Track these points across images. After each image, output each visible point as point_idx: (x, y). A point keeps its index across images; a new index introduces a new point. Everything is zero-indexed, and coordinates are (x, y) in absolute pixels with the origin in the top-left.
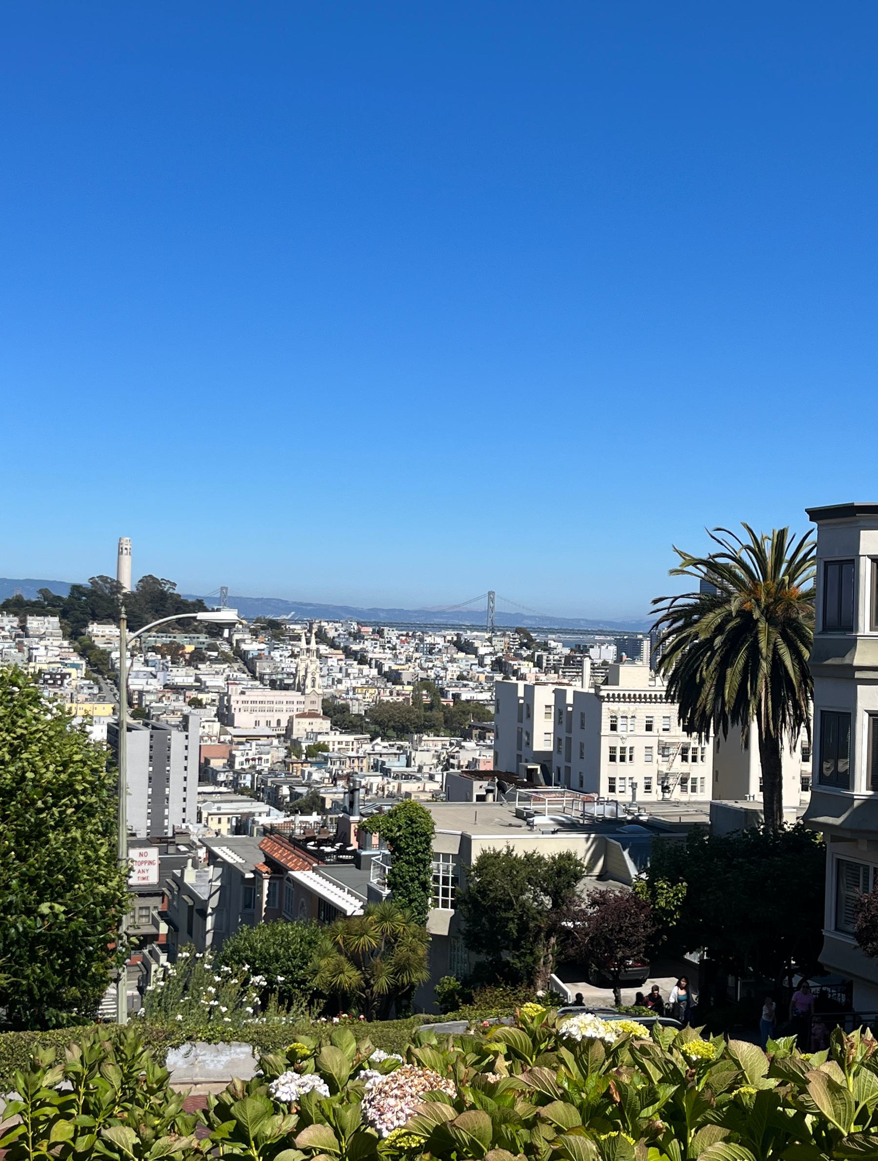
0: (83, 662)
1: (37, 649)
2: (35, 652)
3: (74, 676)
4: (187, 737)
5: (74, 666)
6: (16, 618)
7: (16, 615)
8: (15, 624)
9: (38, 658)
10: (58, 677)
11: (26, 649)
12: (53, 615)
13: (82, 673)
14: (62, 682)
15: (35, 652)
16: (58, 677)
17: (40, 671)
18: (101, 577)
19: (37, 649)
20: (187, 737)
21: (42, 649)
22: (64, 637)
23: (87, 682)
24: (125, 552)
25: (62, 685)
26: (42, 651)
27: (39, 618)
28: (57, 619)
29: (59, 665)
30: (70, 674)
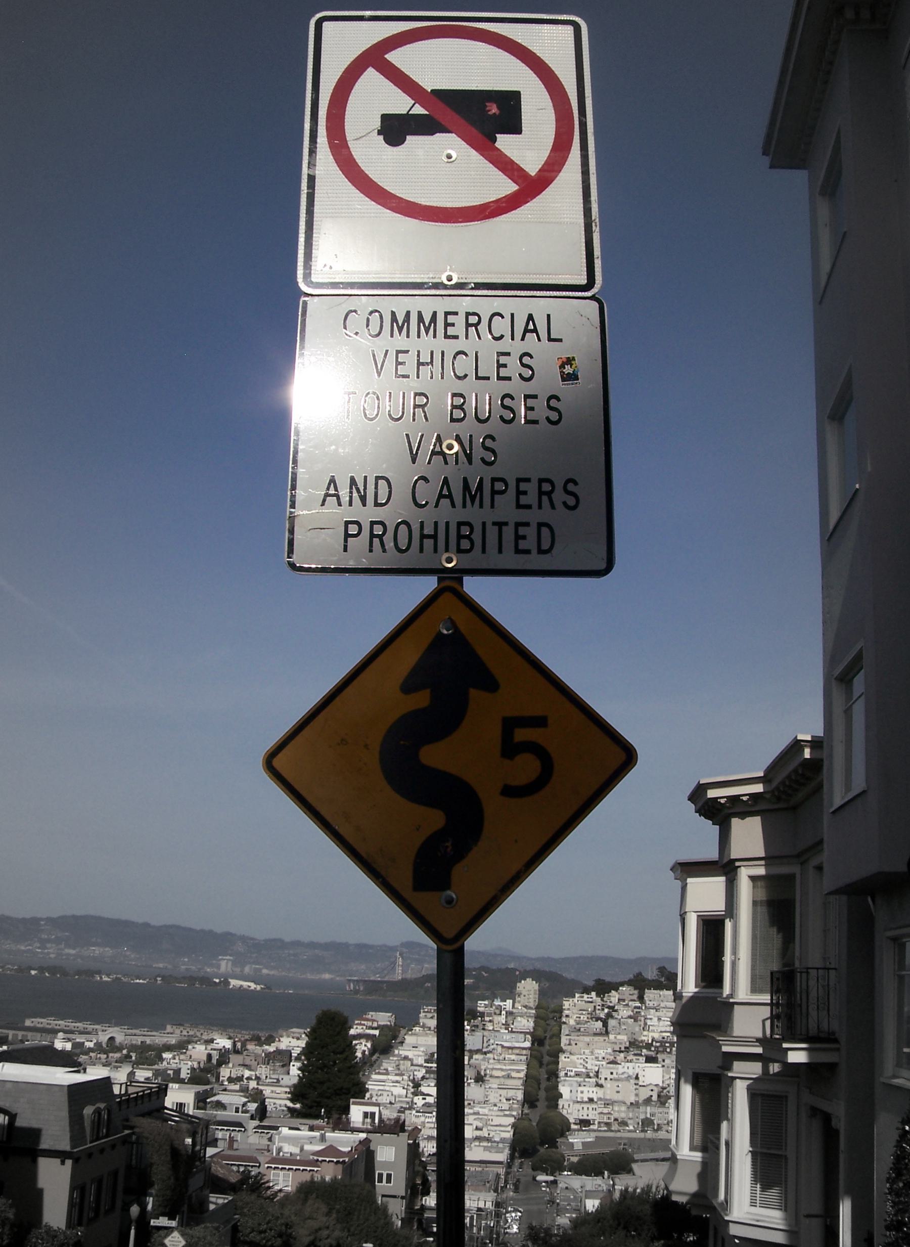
2: (649, 1022)
6: (636, 992)
7: (635, 989)
8: (635, 997)
10: (667, 1045)
11: (643, 1019)
14: (671, 1050)
16: (667, 1045)
17: (652, 1041)
19: (651, 1019)
21: (656, 1019)
26: (655, 1021)
27: (655, 991)
29: (669, 1034)
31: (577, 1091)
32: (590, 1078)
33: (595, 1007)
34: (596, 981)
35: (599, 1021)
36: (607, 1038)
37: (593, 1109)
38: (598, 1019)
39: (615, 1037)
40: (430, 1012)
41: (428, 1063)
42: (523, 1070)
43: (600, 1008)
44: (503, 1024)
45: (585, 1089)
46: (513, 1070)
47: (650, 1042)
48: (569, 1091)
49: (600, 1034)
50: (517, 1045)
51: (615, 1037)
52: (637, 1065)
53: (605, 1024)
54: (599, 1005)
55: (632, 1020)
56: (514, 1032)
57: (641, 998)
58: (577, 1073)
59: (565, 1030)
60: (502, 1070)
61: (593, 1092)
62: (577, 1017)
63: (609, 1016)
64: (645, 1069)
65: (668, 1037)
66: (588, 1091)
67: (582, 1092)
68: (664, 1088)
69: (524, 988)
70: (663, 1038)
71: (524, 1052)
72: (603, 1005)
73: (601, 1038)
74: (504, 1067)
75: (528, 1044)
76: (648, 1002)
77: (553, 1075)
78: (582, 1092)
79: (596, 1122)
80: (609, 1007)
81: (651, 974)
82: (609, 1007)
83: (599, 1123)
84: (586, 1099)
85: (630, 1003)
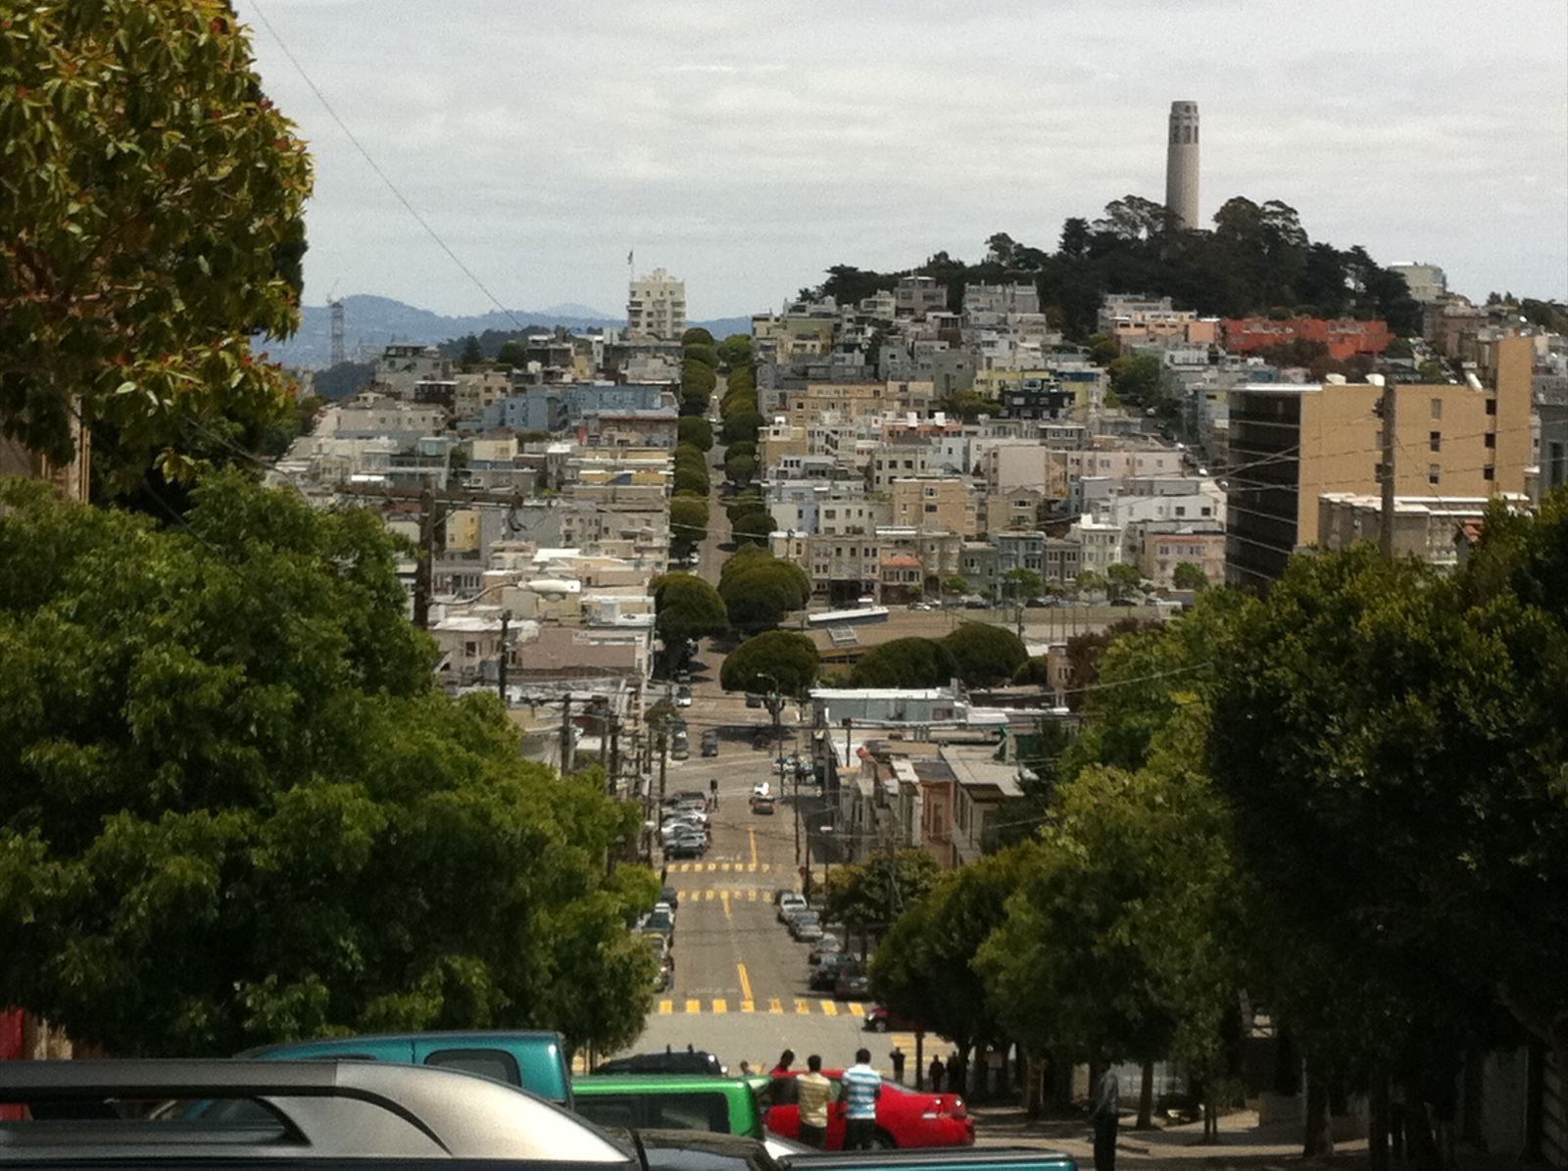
0: (1100, 370)
1: (991, 344)
3: (1078, 400)
4: (1491, 406)
5: (1078, 377)
7: (939, 282)
9: (995, 363)
12: (1024, 281)
13: (1099, 390)
15: (987, 352)
16: (1044, 400)
17: (1003, 391)
18: (1130, 199)
19: (991, 344)
20: (1491, 406)
22: (1052, 326)
23: (1112, 412)
24: (1182, 131)
25: (1054, 415)
28: (1031, 291)
30: (1072, 396)
31: (817, 512)
32: (849, 478)
33: (837, 327)
34: (834, 270)
35: (857, 352)
36: (881, 388)
37: (867, 550)
38: (850, 348)
39: (904, 389)
40: (404, 356)
41: (401, 464)
42: (662, 467)
43: (849, 326)
44: (599, 371)
45: (840, 508)
46: (638, 467)
47: (995, 396)
48: (796, 514)
49: (861, 379)
50: (641, 413)
51: (904, 389)
52: (974, 442)
53: (872, 357)
54: (849, 320)
55: (946, 344)
56: (633, 385)
57: (956, 304)
58: (812, 468)
59: (765, 373)
60: (607, 468)
61: (860, 512)
62: (795, 346)
63: (877, 341)
64: (1002, 452)
65: (1043, 381)
66: (848, 512)
67: (830, 514)
68: (1049, 503)
69: (648, 293)
70: (1032, 384)
71: (665, 429)
72: (861, 320)
73: (868, 390)
74: (610, 461)
75: (671, 412)
76: (974, 313)
77: (745, 471)
78: (830, 514)
79: (877, 588)
80: (874, 322)
81: (973, 253)
82: (874, 322)
83: (885, 589)
84: (841, 531)
85: (930, 315)
